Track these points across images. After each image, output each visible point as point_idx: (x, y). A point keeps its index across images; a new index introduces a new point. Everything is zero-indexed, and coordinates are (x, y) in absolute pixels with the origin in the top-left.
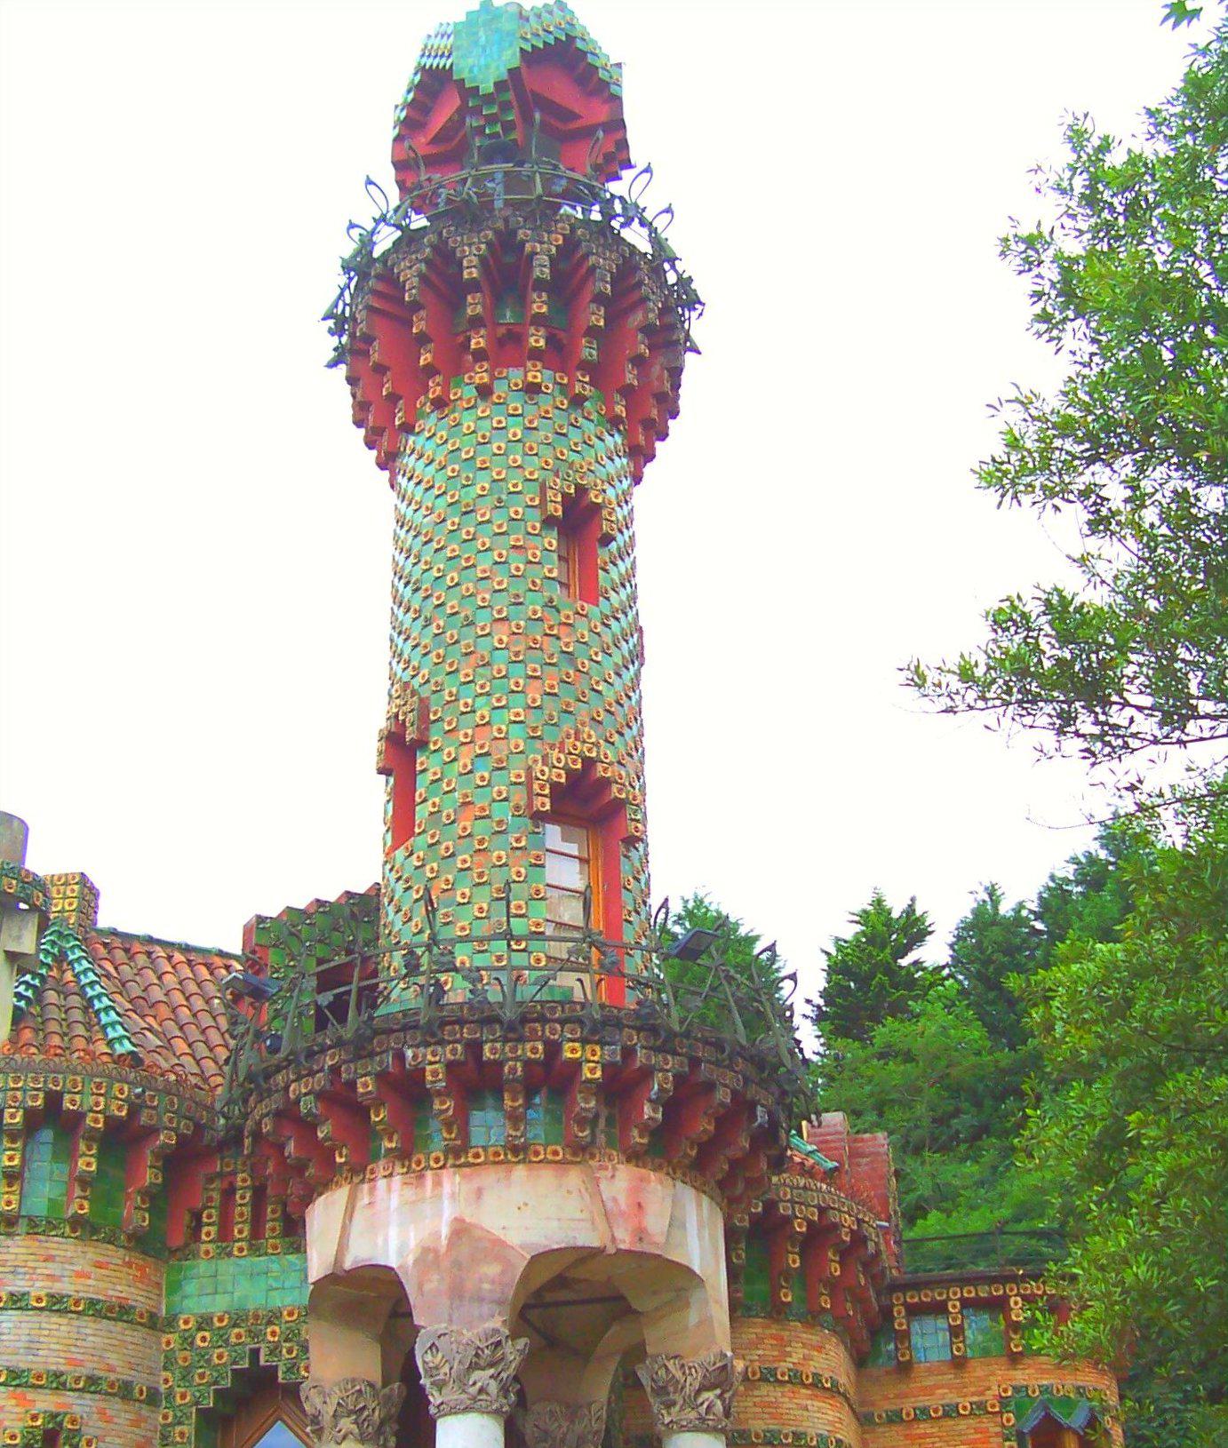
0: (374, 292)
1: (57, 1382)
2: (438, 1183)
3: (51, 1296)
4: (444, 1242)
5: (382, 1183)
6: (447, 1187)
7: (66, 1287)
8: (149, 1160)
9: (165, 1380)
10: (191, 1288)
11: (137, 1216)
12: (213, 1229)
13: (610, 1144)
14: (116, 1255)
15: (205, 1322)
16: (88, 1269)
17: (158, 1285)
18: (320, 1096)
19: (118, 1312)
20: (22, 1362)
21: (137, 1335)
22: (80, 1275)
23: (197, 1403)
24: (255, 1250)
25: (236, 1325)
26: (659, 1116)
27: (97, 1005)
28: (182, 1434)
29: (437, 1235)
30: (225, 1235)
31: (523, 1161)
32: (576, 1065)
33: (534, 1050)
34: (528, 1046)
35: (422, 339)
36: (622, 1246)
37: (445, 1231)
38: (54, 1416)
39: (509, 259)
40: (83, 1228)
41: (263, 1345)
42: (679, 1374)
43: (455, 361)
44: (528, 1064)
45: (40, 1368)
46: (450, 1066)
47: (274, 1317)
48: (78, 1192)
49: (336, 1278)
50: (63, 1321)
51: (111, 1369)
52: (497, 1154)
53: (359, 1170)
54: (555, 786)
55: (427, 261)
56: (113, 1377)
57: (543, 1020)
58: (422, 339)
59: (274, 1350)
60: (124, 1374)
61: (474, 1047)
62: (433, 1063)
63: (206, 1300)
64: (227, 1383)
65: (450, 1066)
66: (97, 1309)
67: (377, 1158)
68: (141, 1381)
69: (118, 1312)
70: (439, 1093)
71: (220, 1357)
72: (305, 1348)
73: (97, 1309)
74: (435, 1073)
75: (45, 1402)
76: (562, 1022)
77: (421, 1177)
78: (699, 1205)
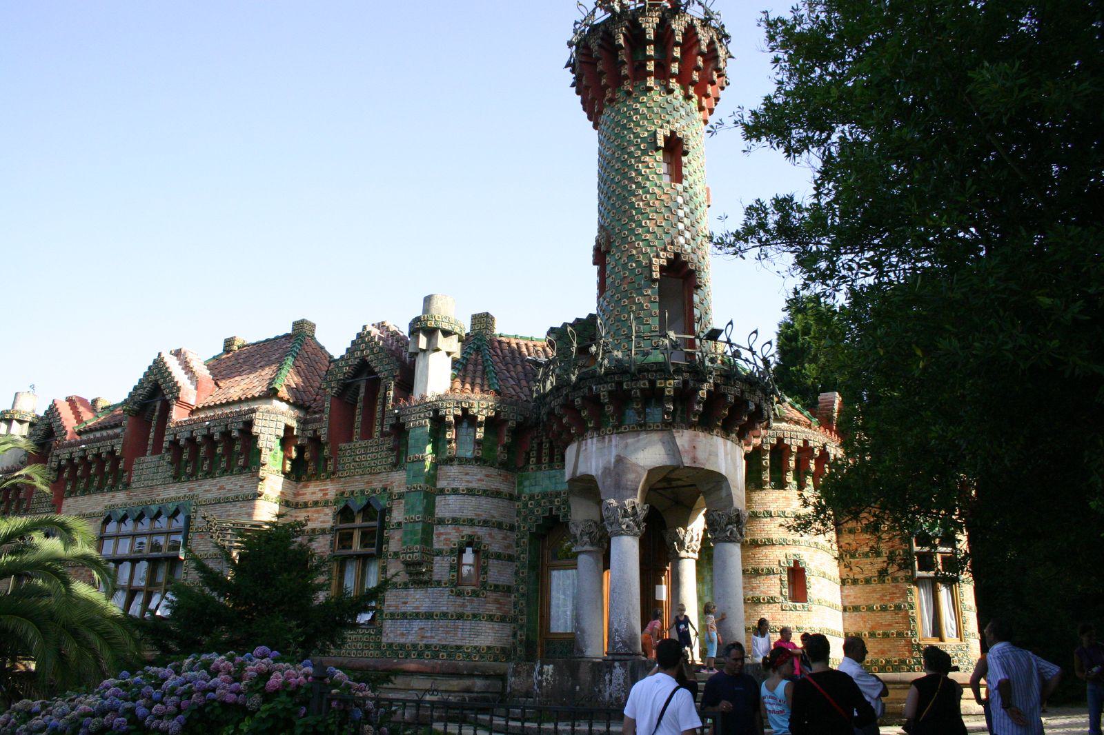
0: (583, 54)
1: (471, 522)
2: (610, 441)
3: (468, 489)
4: (612, 465)
5: (589, 441)
6: (614, 443)
7: (474, 485)
8: (506, 433)
9: (516, 521)
10: (527, 483)
11: (502, 455)
12: (534, 459)
13: (682, 422)
14: (493, 471)
15: (532, 497)
16: (483, 477)
17: (514, 483)
18: (562, 406)
19: (497, 494)
20: (458, 515)
21: (506, 503)
22: (479, 480)
23: (529, 530)
24: (551, 468)
25: (543, 498)
26: (701, 409)
27: (487, 370)
28: (524, 543)
29: (609, 462)
30: (539, 461)
31: (644, 430)
32: (663, 390)
33: (643, 384)
34: (642, 382)
35: (602, 73)
36: (686, 465)
37: (613, 460)
38: (470, 536)
39: (636, 32)
40: (477, 460)
42: (717, 518)
43: (618, 81)
44: (642, 390)
45: (465, 517)
46: (610, 393)
47: (558, 494)
48: (476, 447)
49: (574, 480)
50: (473, 499)
51: (494, 517)
52: (633, 428)
53: (581, 435)
54: (661, 267)
55: (602, 39)
56: (494, 520)
57: (648, 371)
58: (602, 73)
59: (558, 508)
61: (620, 384)
62: (603, 391)
63: (533, 488)
64: (541, 522)
65: (610, 393)
66: (486, 493)
67: (587, 431)
68: (506, 521)
69: (497, 494)
70: (606, 404)
71: (538, 511)
72: (569, 507)
73: (486, 493)
74: (604, 396)
75: (467, 531)
76: (656, 372)
77: (604, 438)
78: (725, 445)
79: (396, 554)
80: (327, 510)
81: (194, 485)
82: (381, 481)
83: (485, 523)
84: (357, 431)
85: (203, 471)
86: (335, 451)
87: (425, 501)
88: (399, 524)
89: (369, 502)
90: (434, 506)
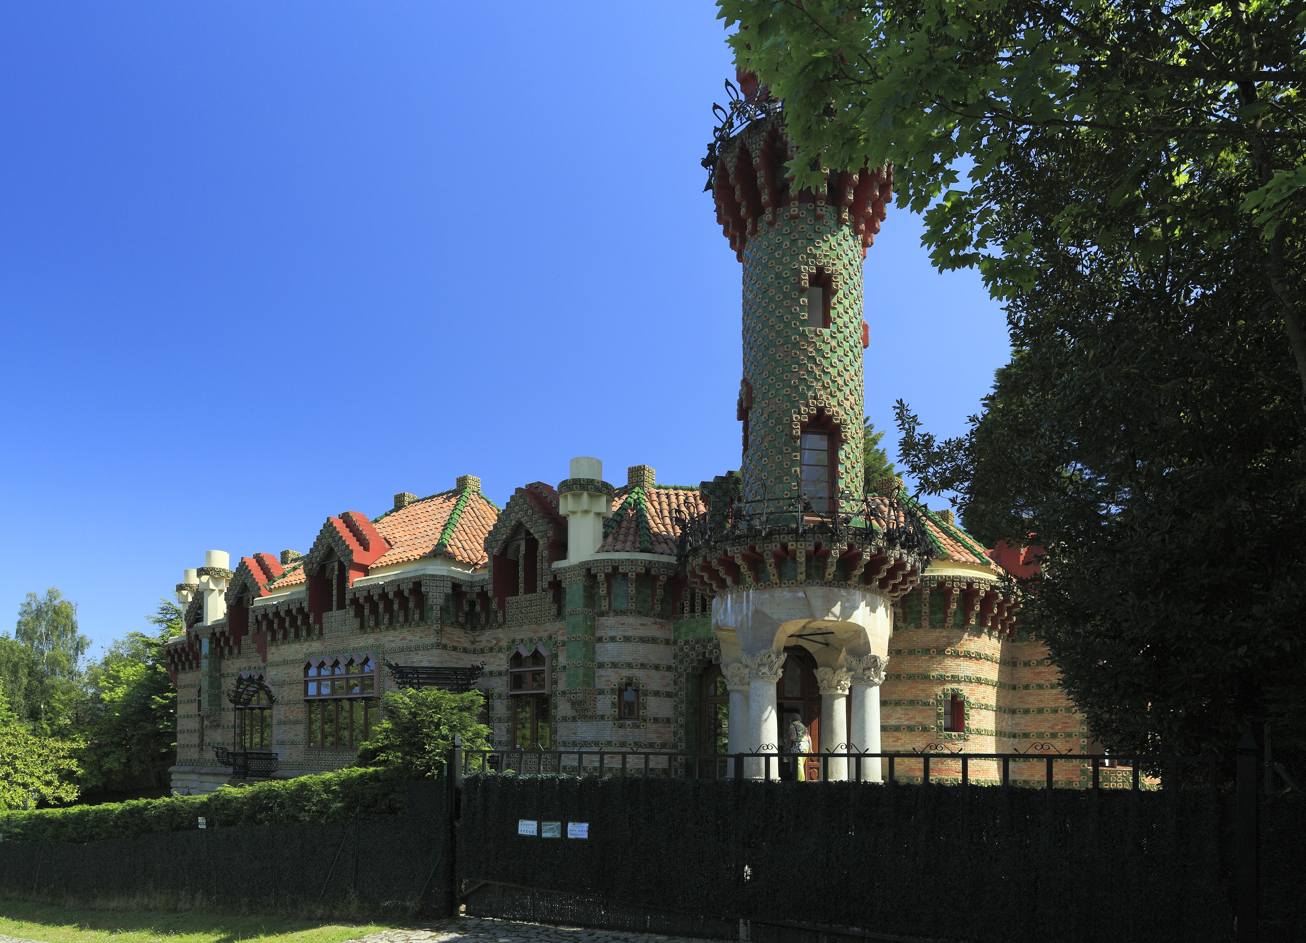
1: (630, 666)
3: (624, 637)
20: (616, 660)
38: (629, 678)
41: (707, 651)
51: (651, 660)
59: (711, 652)
60: (657, 662)
79: (564, 693)
80: (501, 655)
81: (377, 636)
82: (547, 630)
83: (643, 666)
84: (521, 585)
85: (384, 624)
86: (502, 606)
87: (584, 649)
88: (564, 668)
89: (536, 649)
90: (594, 653)
